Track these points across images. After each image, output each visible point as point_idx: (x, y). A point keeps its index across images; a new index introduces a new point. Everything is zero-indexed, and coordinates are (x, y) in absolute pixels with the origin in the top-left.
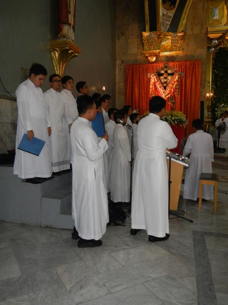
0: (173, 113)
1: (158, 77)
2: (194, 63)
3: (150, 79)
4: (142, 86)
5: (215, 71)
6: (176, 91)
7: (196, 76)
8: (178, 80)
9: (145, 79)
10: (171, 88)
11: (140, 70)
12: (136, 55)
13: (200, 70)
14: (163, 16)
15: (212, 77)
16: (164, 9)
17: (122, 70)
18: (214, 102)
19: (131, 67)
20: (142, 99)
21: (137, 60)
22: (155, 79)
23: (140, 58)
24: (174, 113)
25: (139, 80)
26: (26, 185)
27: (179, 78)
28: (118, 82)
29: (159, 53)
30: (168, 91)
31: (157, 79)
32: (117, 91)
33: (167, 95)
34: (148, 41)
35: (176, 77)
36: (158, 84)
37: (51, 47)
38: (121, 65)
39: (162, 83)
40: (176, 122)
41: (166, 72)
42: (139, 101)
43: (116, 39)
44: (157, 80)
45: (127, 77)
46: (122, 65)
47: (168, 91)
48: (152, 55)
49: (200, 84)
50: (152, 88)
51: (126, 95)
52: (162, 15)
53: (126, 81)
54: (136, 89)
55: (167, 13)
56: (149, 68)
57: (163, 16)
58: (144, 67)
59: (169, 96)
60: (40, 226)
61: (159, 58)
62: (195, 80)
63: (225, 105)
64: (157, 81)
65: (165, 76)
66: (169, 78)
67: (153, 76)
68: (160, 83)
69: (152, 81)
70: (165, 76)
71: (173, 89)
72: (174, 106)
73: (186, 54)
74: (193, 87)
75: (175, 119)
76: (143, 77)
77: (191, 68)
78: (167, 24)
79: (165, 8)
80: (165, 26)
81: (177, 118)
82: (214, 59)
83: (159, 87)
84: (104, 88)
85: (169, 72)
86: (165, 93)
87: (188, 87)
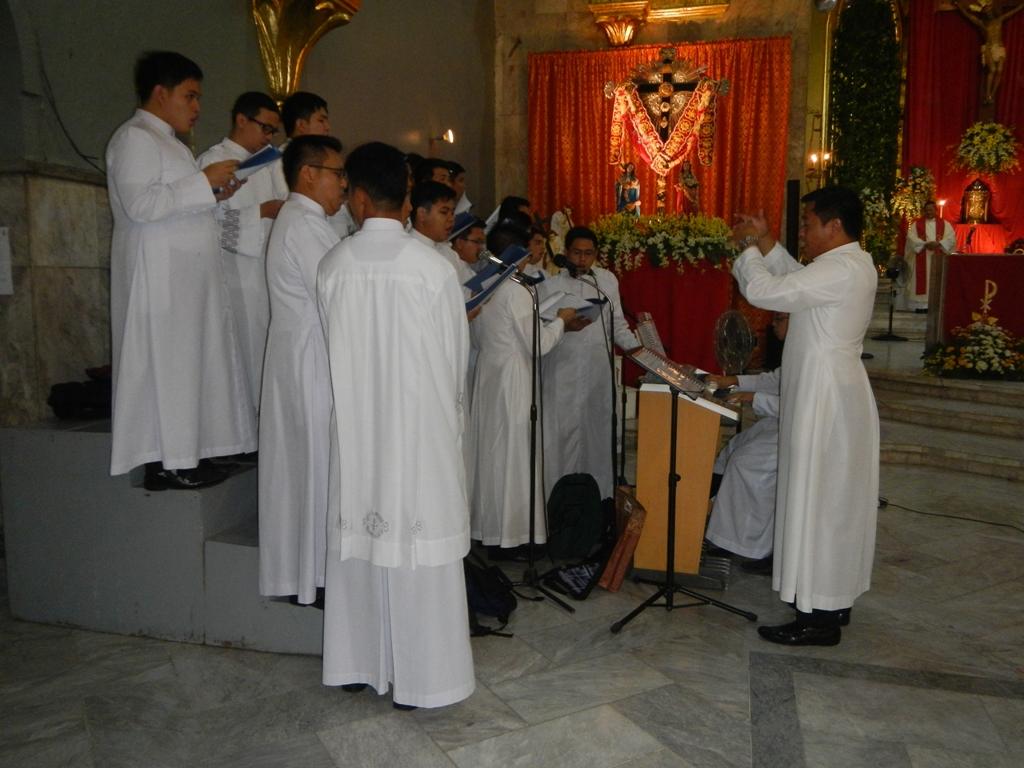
0: (692, 222)
1: (641, 98)
2: (765, 45)
3: (611, 102)
4: (584, 127)
5: (842, 75)
6: (701, 146)
7: (771, 94)
8: (708, 107)
9: (597, 104)
10: (686, 135)
11: (577, 73)
12: (564, 18)
13: (787, 73)
15: (831, 96)
17: (517, 72)
18: (836, 181)
19: (547, 63)
20: (586, 173)
22: (630, 103)
23: (579, 29)
24: (695, 223)
25: (576, 105)
26: (148, 495)
27: (711, 100)
29: (645, 12)
30: (674, 145)
31: (634, 104)
32: (498, 146)
33: (673, 159)
35: (703, 95)
36: (638, 121)
38: (510, 55)
39: (654, 118)
40: (702, 255)
41: (668, 78)
42: (576, 179)
44: (637, 107)
45: (531, 94)
46: (514, 55)
47: (673, 146)
48: (619, 18)
49: (785, 122)
50: (620, 137)
51: (530, 158)
53: (529, 112)
54: (563, 138)
56: (610, 65)
58: (593, 61)
59: (677, 162)
60: (204, 644)
62: (771, 110)
63: (871, 191)
64: (637, 112)
65: (664, 91)
66: (679, 98)
67: (621, 94)
70: (664, 91)
71: (691, 139)
72: (694, 198)
73: (739, 17)
74: (763, 131)
75: (698, 244)
76: (589, 96)
77: (757, 65)
81: (703, 240)
82: (836, 34)
83: (642, 132)
84: (450, 137)
85: (679, 78)
86: (664, 152)
87: (745, 132)
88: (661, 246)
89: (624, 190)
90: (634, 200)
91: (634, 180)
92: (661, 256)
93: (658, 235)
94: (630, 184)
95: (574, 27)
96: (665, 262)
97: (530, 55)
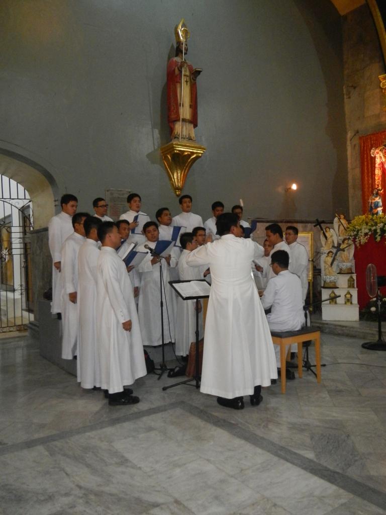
3: (373, 159)
12: (378, 116)
17: (357, 147)
22: (383, 157)
28: (352, 169)
32: (350, 184)
37: (162, 154)
43: (345, 96)
67: (378, 153)
69: (378, 161)
84: (294, 187)
88: (379, 231)
89: (371, 203)
90: (377, 207)
91: (377, 197)
92: (377, 236)
93: (378, 225)
94: (374, 199)
96: (379, 239)
97: (360, 138)
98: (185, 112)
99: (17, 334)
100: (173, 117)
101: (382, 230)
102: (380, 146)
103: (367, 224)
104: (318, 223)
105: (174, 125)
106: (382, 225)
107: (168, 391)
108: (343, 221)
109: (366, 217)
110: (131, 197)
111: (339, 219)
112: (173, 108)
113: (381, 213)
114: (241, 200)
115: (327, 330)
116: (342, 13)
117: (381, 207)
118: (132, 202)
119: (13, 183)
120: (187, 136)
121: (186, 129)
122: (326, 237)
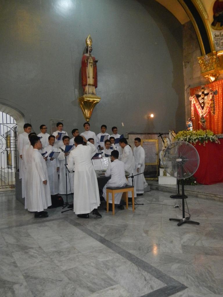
1: (197, 99)
3: (191, 101)
6: (211, 110)
12: (199, 78)
14: (215, 37)
16: (215, 31)
21: (201, 82)
28: (187, 105)
32: (186, 113)
34: (204, 64)
41: (203, 93)
43: (184, 67)
52: (215, 36)
55: (220, 33)
57: (215, 37)
61: (219, 76)
65: (202, 97)
66: (206, 97)
67: (192, 99)
68: (198, 104)
69: (192, 103)
71: (208, 108)
72: (204, 125)
75: (197, 138)
78: (222, 43)
79: (216, 29)
80: (221, 45)
81: (199, 137)
84: (152, 116)
85: (206, 92)
86: (203, 113)
88: (187, 139)
90: (189, 126)
91: (189, 122)
95: (202, 79)
97: (190, 89)
98: (90, 81)
99: (10, 189)
100: (84, 83)
101: (190, 139)
102: (193, 95)
103: (183, 135)
104: (160, 135)
105: (85, 87)
106: (189, 136)
107: (64, 213)
108: (174, 134)
109: (183, 132)
110: (58, 124)
111: (171, 133)
112: (84, 79)
113: (191, 130)
114: (122, 123)
115: (160, 189)
116: (182, 23)
117: (192, 127)
118: (59, 127)
119: (8, 116)
120: (91, 93)
121: (91, 89)
122: (164, 142)
